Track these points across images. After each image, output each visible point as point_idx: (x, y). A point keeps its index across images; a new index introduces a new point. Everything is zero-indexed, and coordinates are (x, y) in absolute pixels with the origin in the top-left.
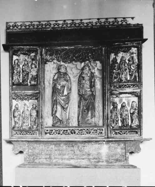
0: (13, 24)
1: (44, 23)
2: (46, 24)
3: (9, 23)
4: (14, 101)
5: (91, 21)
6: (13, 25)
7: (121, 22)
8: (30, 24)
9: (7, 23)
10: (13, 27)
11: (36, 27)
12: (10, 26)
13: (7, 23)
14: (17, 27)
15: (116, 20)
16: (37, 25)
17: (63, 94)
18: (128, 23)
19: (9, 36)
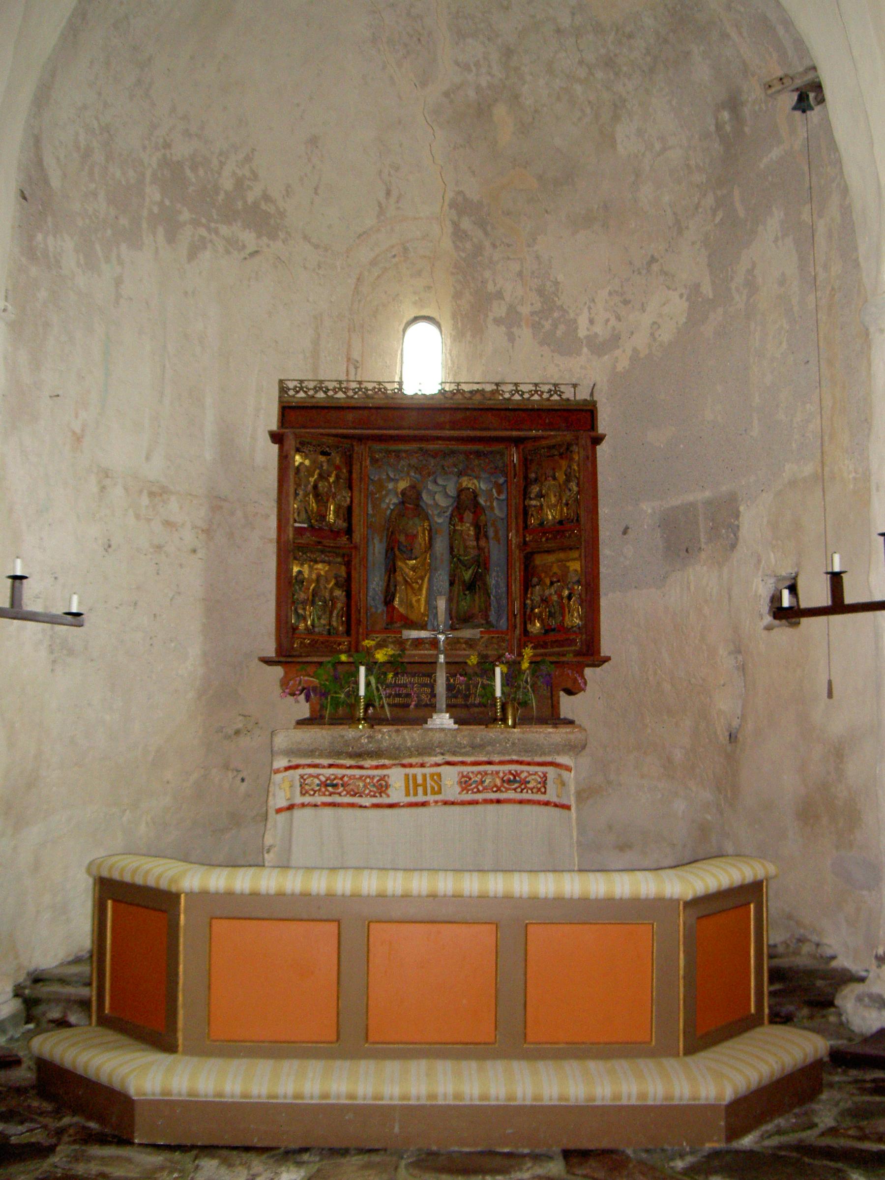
2: (375, 388)
3: (286, 382)
7: (548, 393)
8: (338, 386)
9: (281, 382)
10: (297, 392)
12: (289, 389)
13: (281, 382)
14: (305, 392)
15: (538, 389)
16: (353, 389)
17: (412, 553)
18: (564, 396)
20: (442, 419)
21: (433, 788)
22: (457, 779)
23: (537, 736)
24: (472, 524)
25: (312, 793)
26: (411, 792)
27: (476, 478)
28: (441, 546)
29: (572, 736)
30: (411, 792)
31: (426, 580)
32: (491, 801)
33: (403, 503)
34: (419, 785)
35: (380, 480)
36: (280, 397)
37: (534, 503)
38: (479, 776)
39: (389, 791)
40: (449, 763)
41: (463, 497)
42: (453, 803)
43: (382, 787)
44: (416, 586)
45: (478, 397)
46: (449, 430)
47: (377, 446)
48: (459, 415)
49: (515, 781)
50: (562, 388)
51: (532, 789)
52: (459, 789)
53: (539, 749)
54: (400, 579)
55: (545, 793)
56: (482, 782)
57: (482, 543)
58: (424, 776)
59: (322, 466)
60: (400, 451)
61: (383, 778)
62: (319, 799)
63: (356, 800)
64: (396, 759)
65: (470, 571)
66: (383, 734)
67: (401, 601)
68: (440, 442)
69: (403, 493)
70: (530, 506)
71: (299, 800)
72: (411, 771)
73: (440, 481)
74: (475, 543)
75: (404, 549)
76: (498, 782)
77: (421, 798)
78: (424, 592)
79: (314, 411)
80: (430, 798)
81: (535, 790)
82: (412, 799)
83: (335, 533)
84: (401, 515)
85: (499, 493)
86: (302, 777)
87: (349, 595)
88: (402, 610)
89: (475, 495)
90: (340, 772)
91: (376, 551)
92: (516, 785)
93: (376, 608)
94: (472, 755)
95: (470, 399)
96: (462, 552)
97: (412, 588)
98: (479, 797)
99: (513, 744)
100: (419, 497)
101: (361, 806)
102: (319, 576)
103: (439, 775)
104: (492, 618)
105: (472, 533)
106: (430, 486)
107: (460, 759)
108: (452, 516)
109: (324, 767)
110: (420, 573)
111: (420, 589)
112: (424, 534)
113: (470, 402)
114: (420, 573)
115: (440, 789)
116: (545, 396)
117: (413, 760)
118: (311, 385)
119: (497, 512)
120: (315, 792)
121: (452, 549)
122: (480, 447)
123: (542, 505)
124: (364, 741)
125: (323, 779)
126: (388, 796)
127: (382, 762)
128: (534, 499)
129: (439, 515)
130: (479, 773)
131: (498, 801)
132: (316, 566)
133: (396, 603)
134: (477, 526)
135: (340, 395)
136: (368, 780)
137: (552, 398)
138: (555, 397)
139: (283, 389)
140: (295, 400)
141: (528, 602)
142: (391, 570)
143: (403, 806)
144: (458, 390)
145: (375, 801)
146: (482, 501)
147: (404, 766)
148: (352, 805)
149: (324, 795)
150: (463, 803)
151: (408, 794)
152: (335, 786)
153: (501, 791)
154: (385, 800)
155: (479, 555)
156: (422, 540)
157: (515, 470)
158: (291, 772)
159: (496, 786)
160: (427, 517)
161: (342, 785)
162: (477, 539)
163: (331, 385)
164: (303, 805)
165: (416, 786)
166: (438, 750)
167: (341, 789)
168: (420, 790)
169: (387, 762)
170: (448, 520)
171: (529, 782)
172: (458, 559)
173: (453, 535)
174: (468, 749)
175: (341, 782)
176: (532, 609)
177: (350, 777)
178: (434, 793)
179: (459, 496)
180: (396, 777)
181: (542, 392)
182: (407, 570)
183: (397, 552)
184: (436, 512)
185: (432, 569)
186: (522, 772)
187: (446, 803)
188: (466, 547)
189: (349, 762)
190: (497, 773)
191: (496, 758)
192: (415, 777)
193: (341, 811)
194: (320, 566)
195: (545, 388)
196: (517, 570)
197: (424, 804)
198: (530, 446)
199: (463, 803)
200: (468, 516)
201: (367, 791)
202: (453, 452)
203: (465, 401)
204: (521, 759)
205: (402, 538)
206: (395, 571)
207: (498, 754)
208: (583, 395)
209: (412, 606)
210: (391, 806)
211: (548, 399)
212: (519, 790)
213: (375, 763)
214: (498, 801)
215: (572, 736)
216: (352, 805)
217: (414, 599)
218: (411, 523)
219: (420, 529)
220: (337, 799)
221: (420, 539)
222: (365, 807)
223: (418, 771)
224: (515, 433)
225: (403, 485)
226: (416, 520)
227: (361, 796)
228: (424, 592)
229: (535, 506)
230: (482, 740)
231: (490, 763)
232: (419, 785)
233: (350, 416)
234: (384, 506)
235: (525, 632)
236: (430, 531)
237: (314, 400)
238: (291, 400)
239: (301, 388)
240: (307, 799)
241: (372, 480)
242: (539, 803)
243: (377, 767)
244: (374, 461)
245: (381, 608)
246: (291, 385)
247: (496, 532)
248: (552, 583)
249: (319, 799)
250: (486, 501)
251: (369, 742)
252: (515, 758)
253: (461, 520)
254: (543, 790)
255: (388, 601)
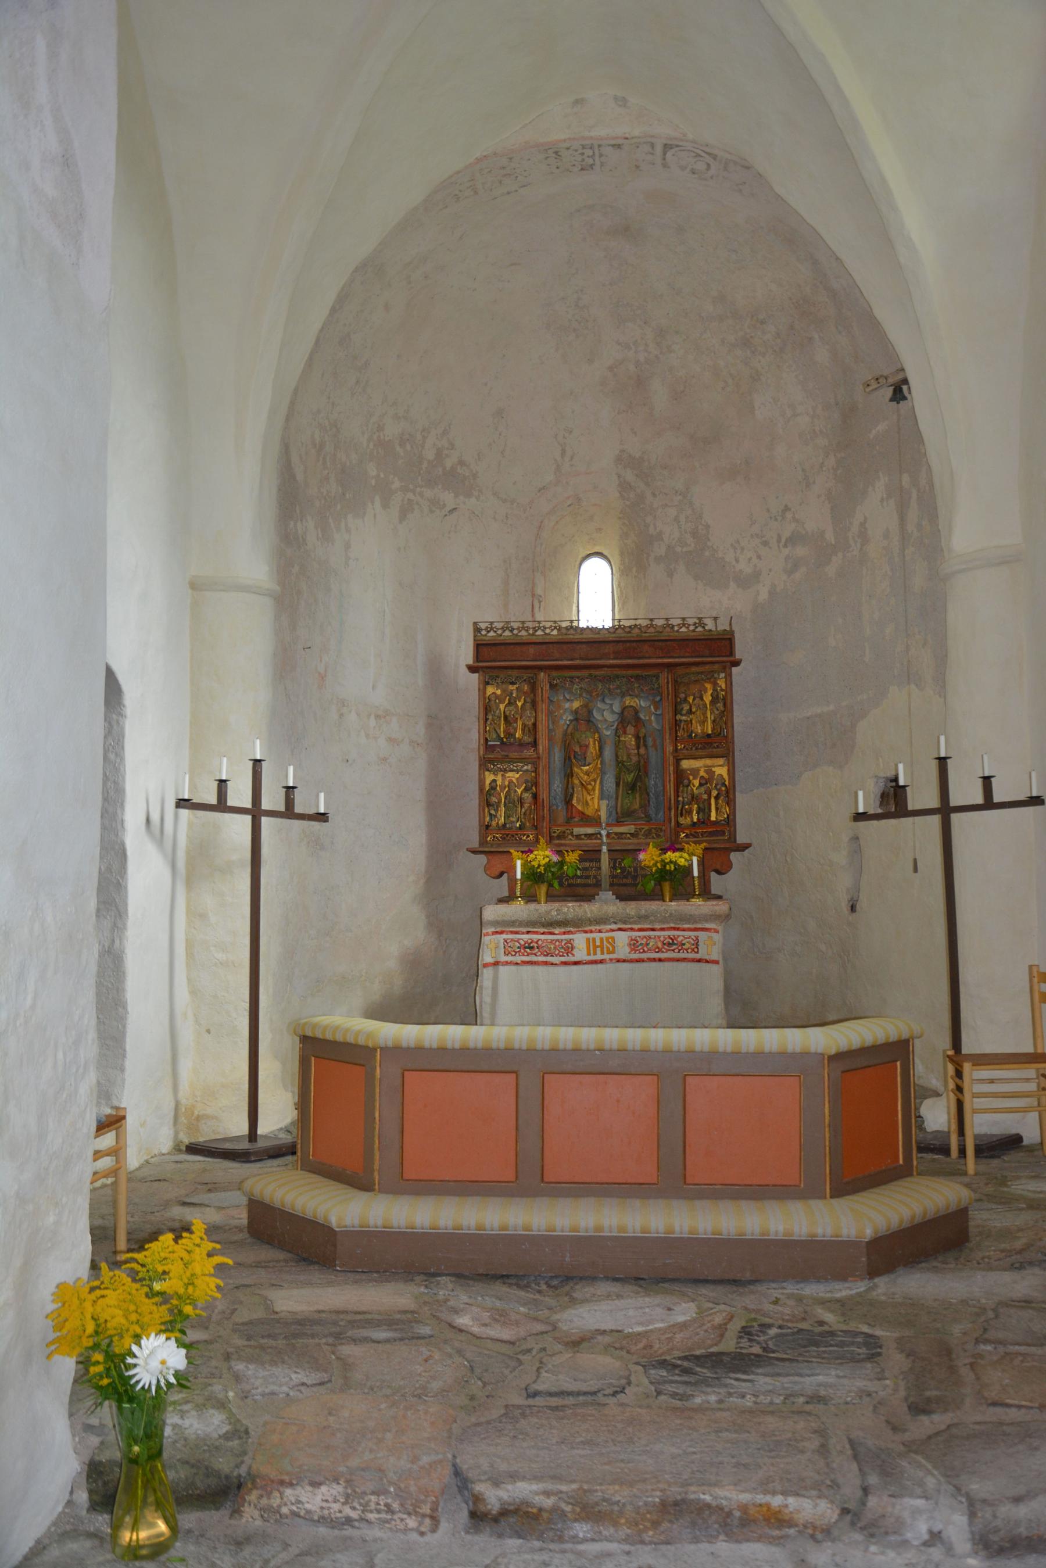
0: (487, 624)
1: (548, 625)
2: (551, 626)
4: (487, 773)
5: (638, 622)
6: (487, 627)
9: (475, 624)
10: (488, 632)
11: (531, 631)
13: (475, 624)
18: (707, 628)
19: (480, 647)
20: (607, 651)
21: (608, 948)
22: (627, 941)
23: (690, 908)
24: (633, 735)
25: (513, 953)
26: (592, 952)
27: (636, 696)
28: (608, 753)
29: (716, 908)
30: (592, 952)
31: (598, 782)
32: (654, 960)
33: (576, 719)
34: (598, 947)
35: (558, 700)
36: (475, 636)
37: (684, 718)
38: (645, 940)
39: (575, 952)
40: (620, 929)
41: (626, 713)
42: (624, 961)
43: (569, 949)
44: (590, 787)
45: (636, 631)
46: (613, 659)
47: (554, 674)
48: (620, 647)
49: (673, 944)
50: (706, 621)
51: (687, 950)
52: (627, 949)
53: (691, 919)
54: (576, 782)
55: (698, 952)
56: (647, 944)
57: (642, 751)
58: (601, 939)
59: (512, 694)
60: (572, 678)
61: (569, 941)
62: (518, 959)
63: (549, 959)
64: (579, 927)
65: (632, 774)
66: (568, 907)
67: (578, 801)
68: (606, 669)
69: (576, 712)
70: (681, 721)
71: (504, 958)
72: (589, 935)
73: (608, 701)
74: (636, 751)
75: (579, 757)
76: (660, 945)
77: (599, 957)
78: (597, 792)
79: (503, 647)
80: (606, 957)
81: (689, 951)
82: (592, 958)
83: (522, 745)
84: (576, 729)
85: (656, 709)
86: (505, 941)
87: (535, 796)
88: (580, 808)
89: (637, 712)
90: (535, 937)
91: (556, 758)
92: (674, 947)
93: (558, 806)
94: (639, 923)
95: (629, 632)
96: (625, 759)
97: (587, 789)
98: (644, 956)
99: (671, 914)
100: (590, 712)
101: (552, 964)
102: (511, 782)
103: (613, 938)
104: (652, 812)
105: (633, 743)
106: (600, 705)
107: (629, 926)
108: (617, 729)
109: (523, 933)
110: (594, 776)
111: (594, 789)
112: (595, 744)
113: (629, 635)
114: (594, 776)
115: (614, 948)
116: (692, 628)
117: (593, 928)
118: (500, 625)
119: (654, 724)
120: (516, 952)
121: (617, 756)
122: (638, 672)
123: (691, 721)
124: (554, 913)
125: (522, 942)
126: (573, 955)
127: (568, 929)
128: (685, 715)
129: (607, 729)
130: (645, 937)
131: (660, 960)
132: (507, 775)
133: (574, 802)
134: (637, 737)
135: (523, 633)
136: (557, 943)
137: (697, 630)
138: (700, 629)
139: (477, 630)
140: (487, 638)
141: (680, 799)
142: (569, 775)
143: (586, 963)
144: (620, 626)
145: (563, 959)
146: (642, 716)
147: (586, 932)
148: (546, 963)
149: (524, 955)
150: (632, 961)
151: (589, 954)
152: (532, 948)
153: (663, 952)
154: (571, 959)
155: (639, 762)
156: (593, 749)
157: (668, 691)
158: (498, 936)
159: (658, 948)
160: (597, 730)
161: (538, 948)
162: (638, 748)
163: (515, 625)
164: (507, 963)
165: (595, 947)
166: (612, 920)
167: (537, 950)
168: (598, 950)
169: (572, 929)
170: (614, 732)
171: (684, 944)
172: (623, 765)
173: (618, 744)
174: (636, 919)
175: (536, 945)
176: (684, 805)
177: (543, 941)
178: (609, 952)
179: (622, 712)
180: (580, 940)
181: (689, 625)
182: (582, 775)
183: (574, 761)
184: (605, 727)
185: (603, 773)
186: (679, 936)
187: (618, 961)
188: (629, 755)
189: (542, 930)
190: (659, 937)
191: (658, 926)
192: (594, 940)
193: (536, 968)
194: (510, 774)
195: (691, 621)
196: (671, 772)
197: (601, 962)
198: (680, 671)
199: (632, 961)
200: (630, 729)
201: (557, 952)
202: (617, 677)
203: (625, 635)
204: (677, 926)
205: (577, 749)
206: (572, 776)
207: (659, 922)
208: (723, 626)
209: (587, 804)
210: (576, 963)
211: (694, 631)
212: (677, 951)
213: (563, 930)
214: (660, 960)
215: (716, 908)
216: (546, 963)
217: (589, 798)
218: (584, 736)
219: (591, 740)
220: (534, 958)
221: (591, 749)
222: (556, 964)
223: (597, 936)
224: (666, 660)
225: (576, 704)
226: (588, 734)
227: (552, 956)
228: (597, 792)
229: (685, 721)
230: (646, 911)
231: (653, 930)
232: (598, 947)
233: (532, 650)
234: (562, 722)
235: (678, 824)
236: (600, 741)
237: (502, 638)
238: (484, 638)
239: (492, 629)
240: (509, 958)
241: (551, 701)
242: (693, 960)
243: (564, 933)
244: (552, 686)
245: (561, 806)
246: (483, 626)
247: (654, 741)
248: (701, 785)
249: (518, 959)
250: (645, 716)
251: (558, 914)
252: (672, 925)
253: (625, 733)
254: (696, 950)
255: (568, 801)
